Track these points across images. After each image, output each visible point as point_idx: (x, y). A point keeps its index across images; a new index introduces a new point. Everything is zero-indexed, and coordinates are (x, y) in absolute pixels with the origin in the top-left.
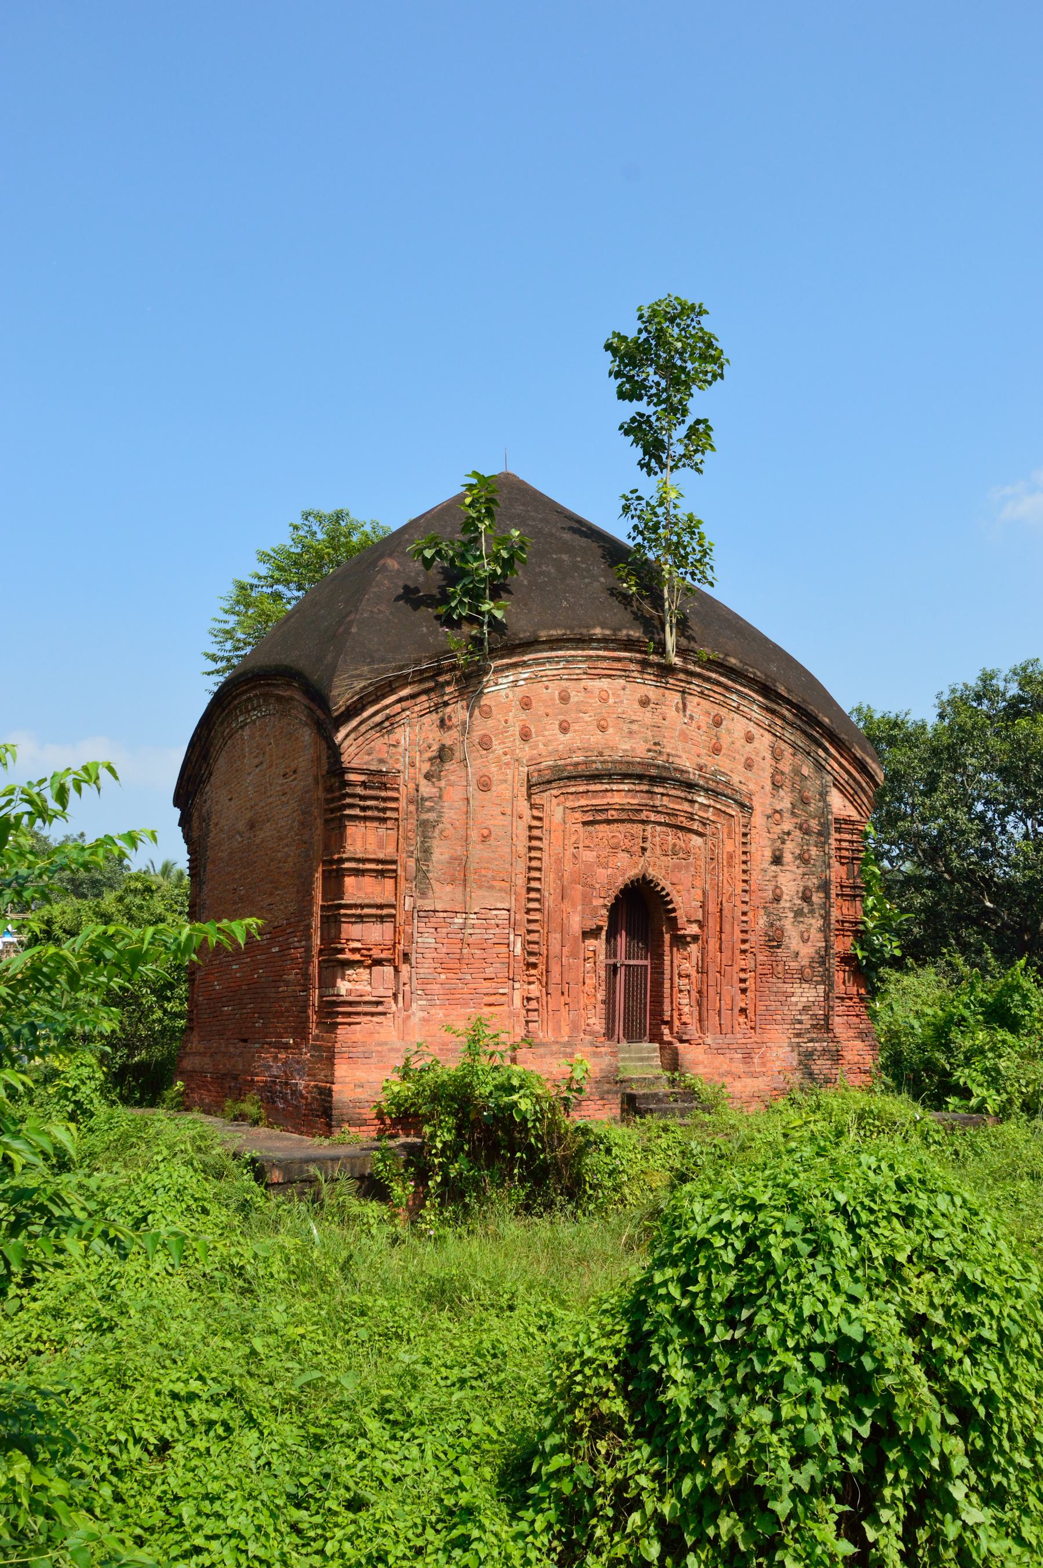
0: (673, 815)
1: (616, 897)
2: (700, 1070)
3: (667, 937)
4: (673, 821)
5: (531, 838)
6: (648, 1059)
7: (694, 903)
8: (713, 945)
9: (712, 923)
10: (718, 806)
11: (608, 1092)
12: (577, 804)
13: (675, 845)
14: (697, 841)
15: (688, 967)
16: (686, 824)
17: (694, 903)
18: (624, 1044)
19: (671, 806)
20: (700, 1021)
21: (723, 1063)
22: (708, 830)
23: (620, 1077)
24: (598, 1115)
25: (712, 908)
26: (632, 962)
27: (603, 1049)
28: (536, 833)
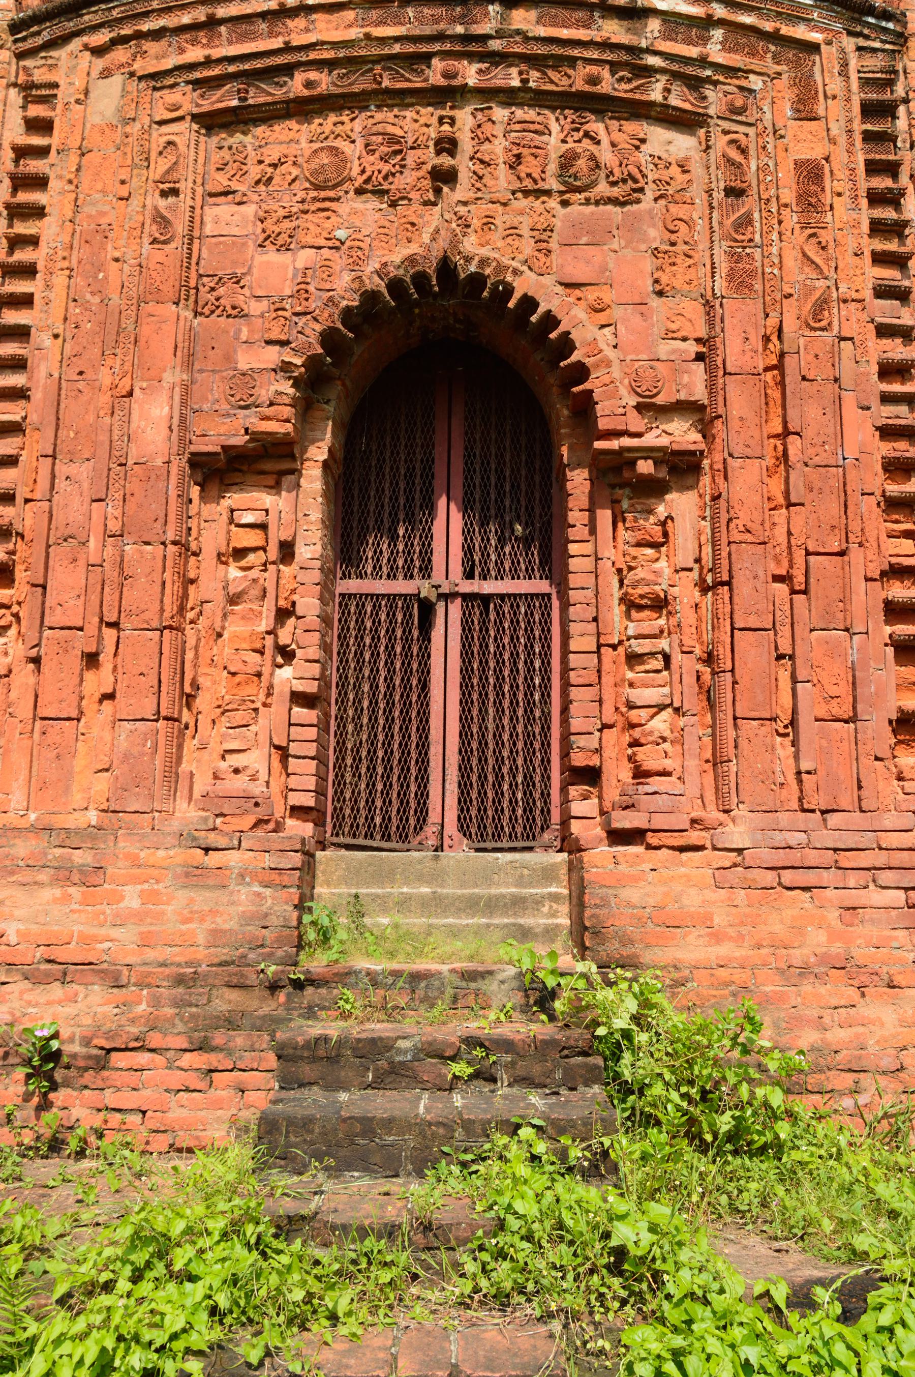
0: (560, 62)
1: (329, 338)
2: (692, 949)
3: (578, 481)
4: (558, 81)
5: (20, 182)
6: (518, 903)
7: (665, 349)
8: (748, 485)
9: (740, 402)
10: (747, 19)
11: (230, 1023)
12: (169, 63)
13: (567, 161)
14: (662, 141)
15: (659, 572)
16: (608, 84)
17: (665, 349)
18: (460, 854)
19: (542, 31)
20: (717, 762)
21: (810, 926)
22: (715, 101)
23: (316, 962)
24: (179, 1111)
25: (737, 351)
26: (489, 587)
27: (233, 858)
28: (34, 166)
